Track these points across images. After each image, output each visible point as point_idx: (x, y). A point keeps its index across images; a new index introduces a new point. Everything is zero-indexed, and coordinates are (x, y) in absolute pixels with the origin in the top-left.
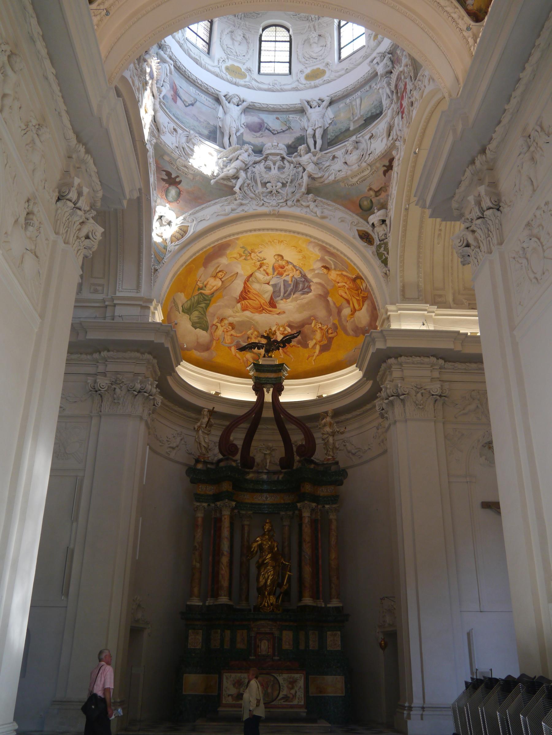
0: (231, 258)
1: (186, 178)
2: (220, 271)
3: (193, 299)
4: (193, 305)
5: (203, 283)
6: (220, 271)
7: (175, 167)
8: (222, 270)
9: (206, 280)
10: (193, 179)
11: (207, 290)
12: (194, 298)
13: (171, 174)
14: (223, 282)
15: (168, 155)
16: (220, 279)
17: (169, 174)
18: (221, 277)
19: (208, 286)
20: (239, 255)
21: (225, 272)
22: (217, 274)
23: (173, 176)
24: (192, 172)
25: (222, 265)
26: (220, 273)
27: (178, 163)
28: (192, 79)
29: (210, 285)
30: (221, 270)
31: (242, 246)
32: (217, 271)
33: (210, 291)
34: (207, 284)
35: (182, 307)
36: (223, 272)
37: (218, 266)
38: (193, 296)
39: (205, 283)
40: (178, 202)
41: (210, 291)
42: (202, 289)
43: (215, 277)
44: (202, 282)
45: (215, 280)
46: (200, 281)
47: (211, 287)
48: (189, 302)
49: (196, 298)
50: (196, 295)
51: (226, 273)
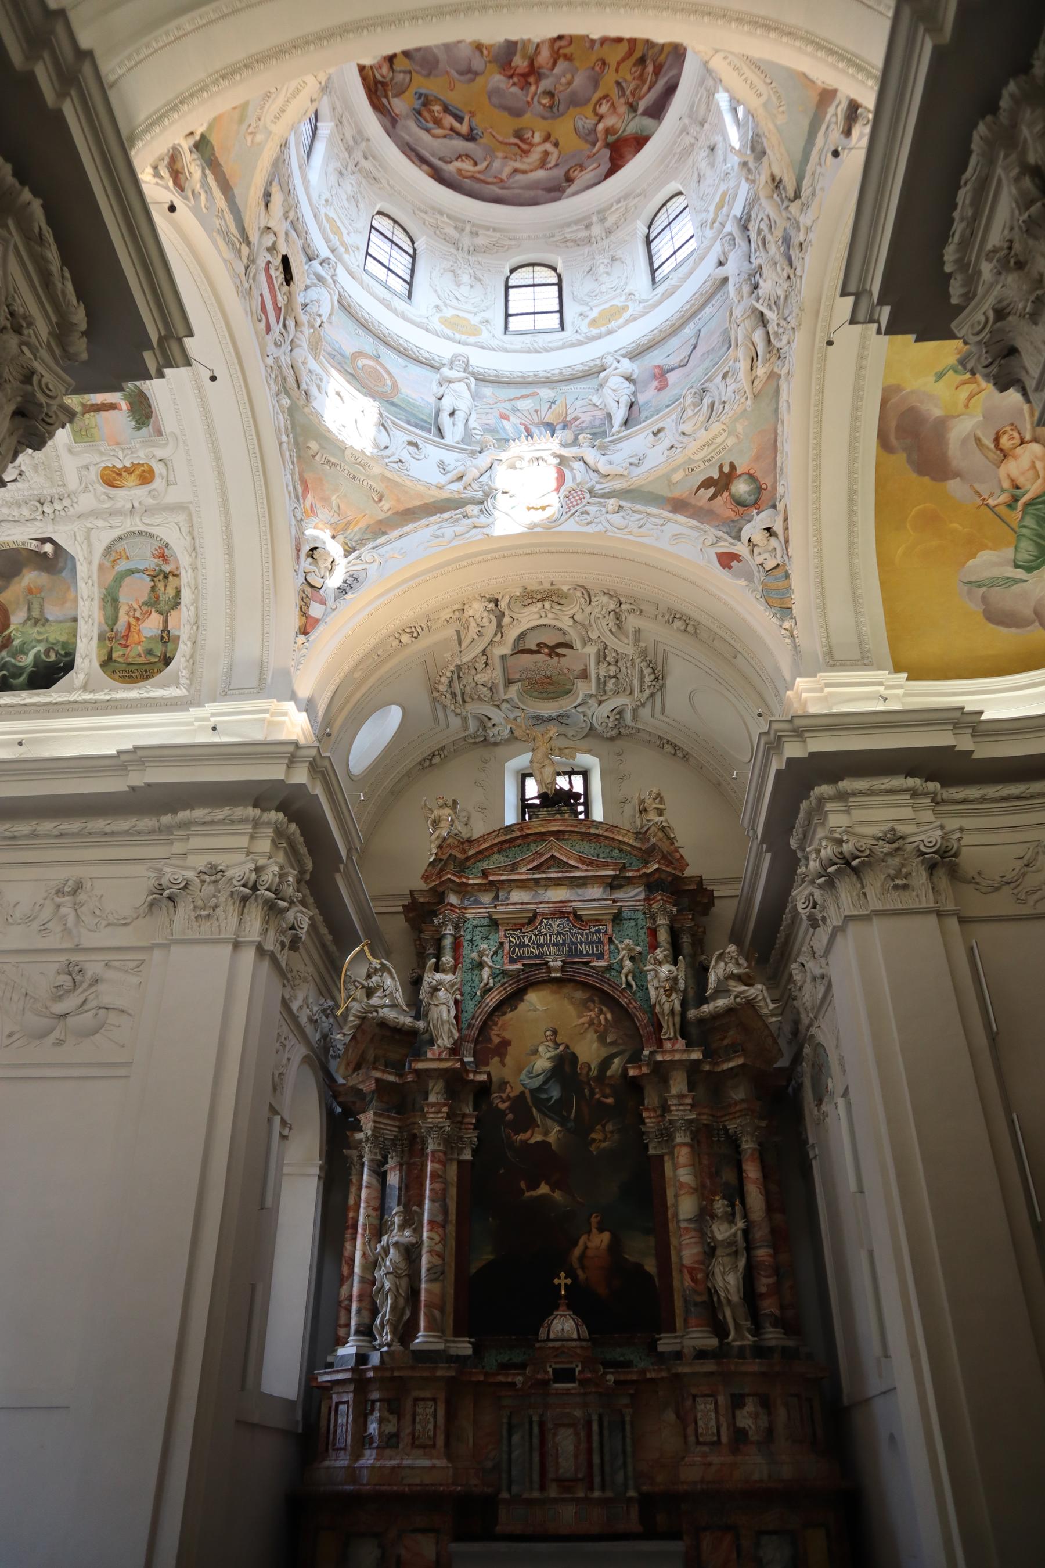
0: (967, 406)
1: (730, 450)
2: (997, 440)
3: (1024, 531)
4: (1041, 537)
5: (1003, 490)
6: (997, 440)
7: (703, 466)
8: (997, 433)
9: (1000, 481)
10: (738, 437)
11: (1028, 487)
12: (1024, 527)
13: (711, 478)
14: (1035, 440)
15: (674, 470)
16: (1022, 443)
17: (708, 483)
18: (1017, 441)
19: (1021, 481)
20: (966, 386)
21: (1008, 428)
22: (1001, 450)
23: (716, 476)
24: (725, 434)
25: (979, 434)
26: (1004, 441)
27: (696, 458)
28: (678, 319)
29: (1023, 473)
30: (993, 437)
31: (933, 379)
32: (992, 446)
33: (1040, 481)
34: (1012, 481)
35: (1017, 566)
36: (1005, 433)
37: (978, 440)
38: (1017, 529)
39: (1006, 484)
40: (764, 486)
41: (1040, 481)
42: (1016, 499)
43: (1005, 456)
44: (998, 492)
45: (1015, 457)
46: (991, 495)
47: (1031, 473)
48: (1025, 544)
49: (1030, 521)
50: (1022, 518)
51: (1012, 424)
